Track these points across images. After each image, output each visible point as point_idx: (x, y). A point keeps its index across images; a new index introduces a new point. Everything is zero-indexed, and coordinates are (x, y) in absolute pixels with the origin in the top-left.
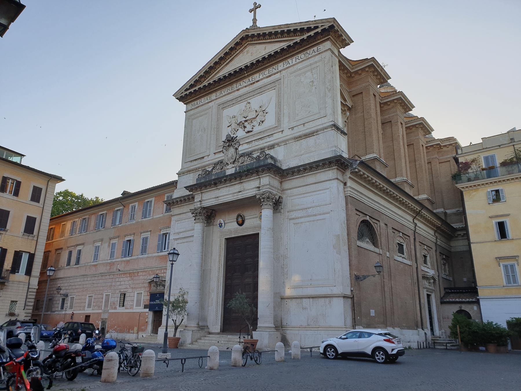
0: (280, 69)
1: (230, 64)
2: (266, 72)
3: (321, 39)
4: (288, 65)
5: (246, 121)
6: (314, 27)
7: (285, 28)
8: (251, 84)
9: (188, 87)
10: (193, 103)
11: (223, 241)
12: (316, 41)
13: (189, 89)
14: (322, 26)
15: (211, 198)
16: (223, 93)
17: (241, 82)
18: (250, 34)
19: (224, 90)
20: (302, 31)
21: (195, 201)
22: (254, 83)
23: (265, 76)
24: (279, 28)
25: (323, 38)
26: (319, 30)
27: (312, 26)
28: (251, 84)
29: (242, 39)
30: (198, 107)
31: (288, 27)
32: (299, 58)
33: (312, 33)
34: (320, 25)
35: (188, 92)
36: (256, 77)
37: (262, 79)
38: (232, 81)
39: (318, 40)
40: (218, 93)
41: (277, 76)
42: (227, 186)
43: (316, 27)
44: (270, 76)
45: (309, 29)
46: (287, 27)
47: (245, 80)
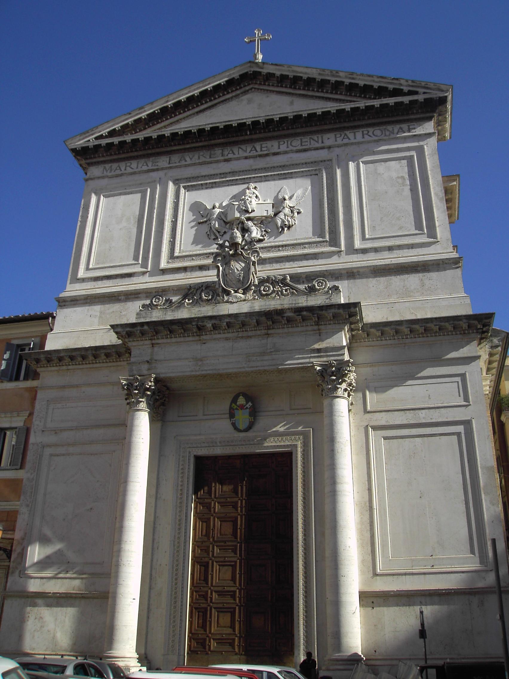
0: (327, 143)
1: (208, 113)
2: (296, 143)
3: (417, 113)
4: (346, 141)
5: (249, 219)
6: (409, 91)
7: (346, 77)
8: (260, 156)
9: (105, 132)
10: (108, 166)
11: (192, 460)
12: (408, 114)
13: (106, 137)
14: (424, 93)
15: (177, 360)
16: (188, 159)
17: (235, 149)
18: (264, 71)
19: (191, 154)
20: (382, 92)
21: (132, 360)
22: (267, 155)
23: (291, 148)
24: (333, 76)
25: (422, 113)
26: (420, 98)
27: (406, 89)
28: (260, 156)
29: (244, 77)
30: (122, 175)
31: (353, 79)
32: (370, 134)
33: (406, 99)
34: (421, 90)
35: (104, 142)
36: (273, 146)
37: (286, 153)
38: (213, 142)
39: (413, 113)
40: (175, 158)
41: (323, 154)
42: (227, 339)
43: (416, 93)
44: (305, 150)
45: (397, 92)
46: (350, 78)
47: (243, 147)
